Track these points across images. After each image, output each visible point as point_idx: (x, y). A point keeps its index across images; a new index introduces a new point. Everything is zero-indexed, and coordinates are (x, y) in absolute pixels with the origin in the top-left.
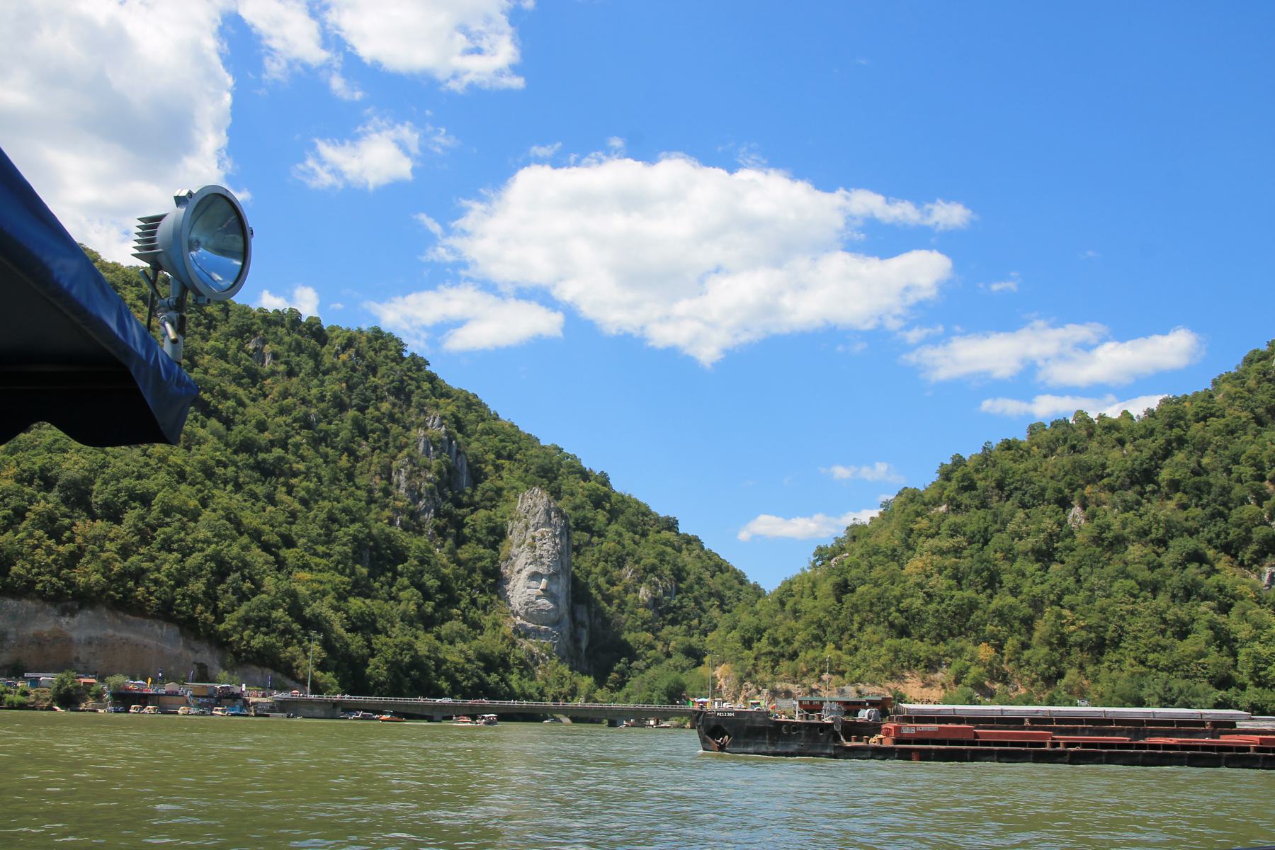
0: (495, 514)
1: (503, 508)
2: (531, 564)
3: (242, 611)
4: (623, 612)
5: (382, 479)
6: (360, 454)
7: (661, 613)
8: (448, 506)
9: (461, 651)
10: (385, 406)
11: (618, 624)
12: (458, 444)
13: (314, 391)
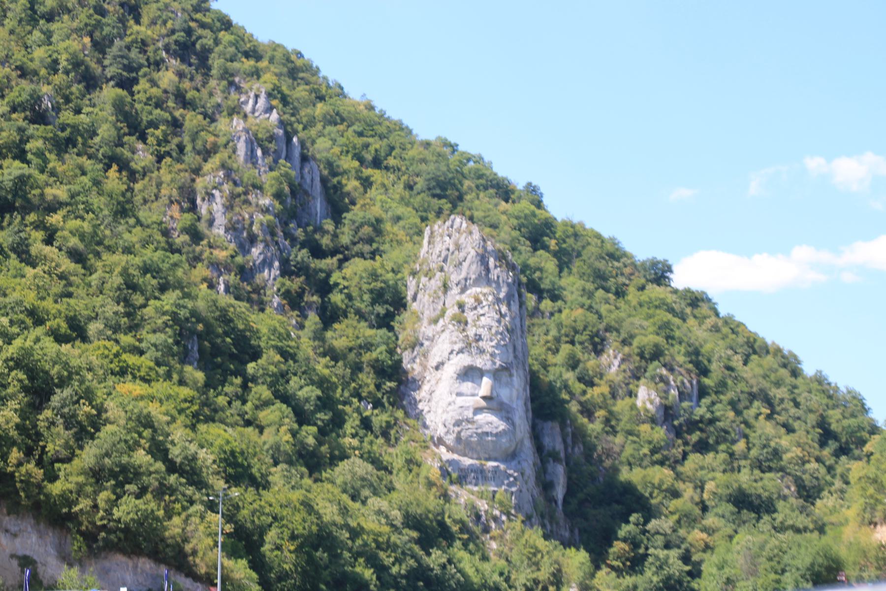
0: (383, 266)
1: (392, 256)
2: (461, 351)
3: (88, 455)
4: (615, 432)
5: (182, 210)
6: (136, 166)
7: (678, 432)
8: (303, 254)
9: (379, 512)
10: (167, 78)
11: (609, 453)
12: (302, 143)
13: (39, 53)
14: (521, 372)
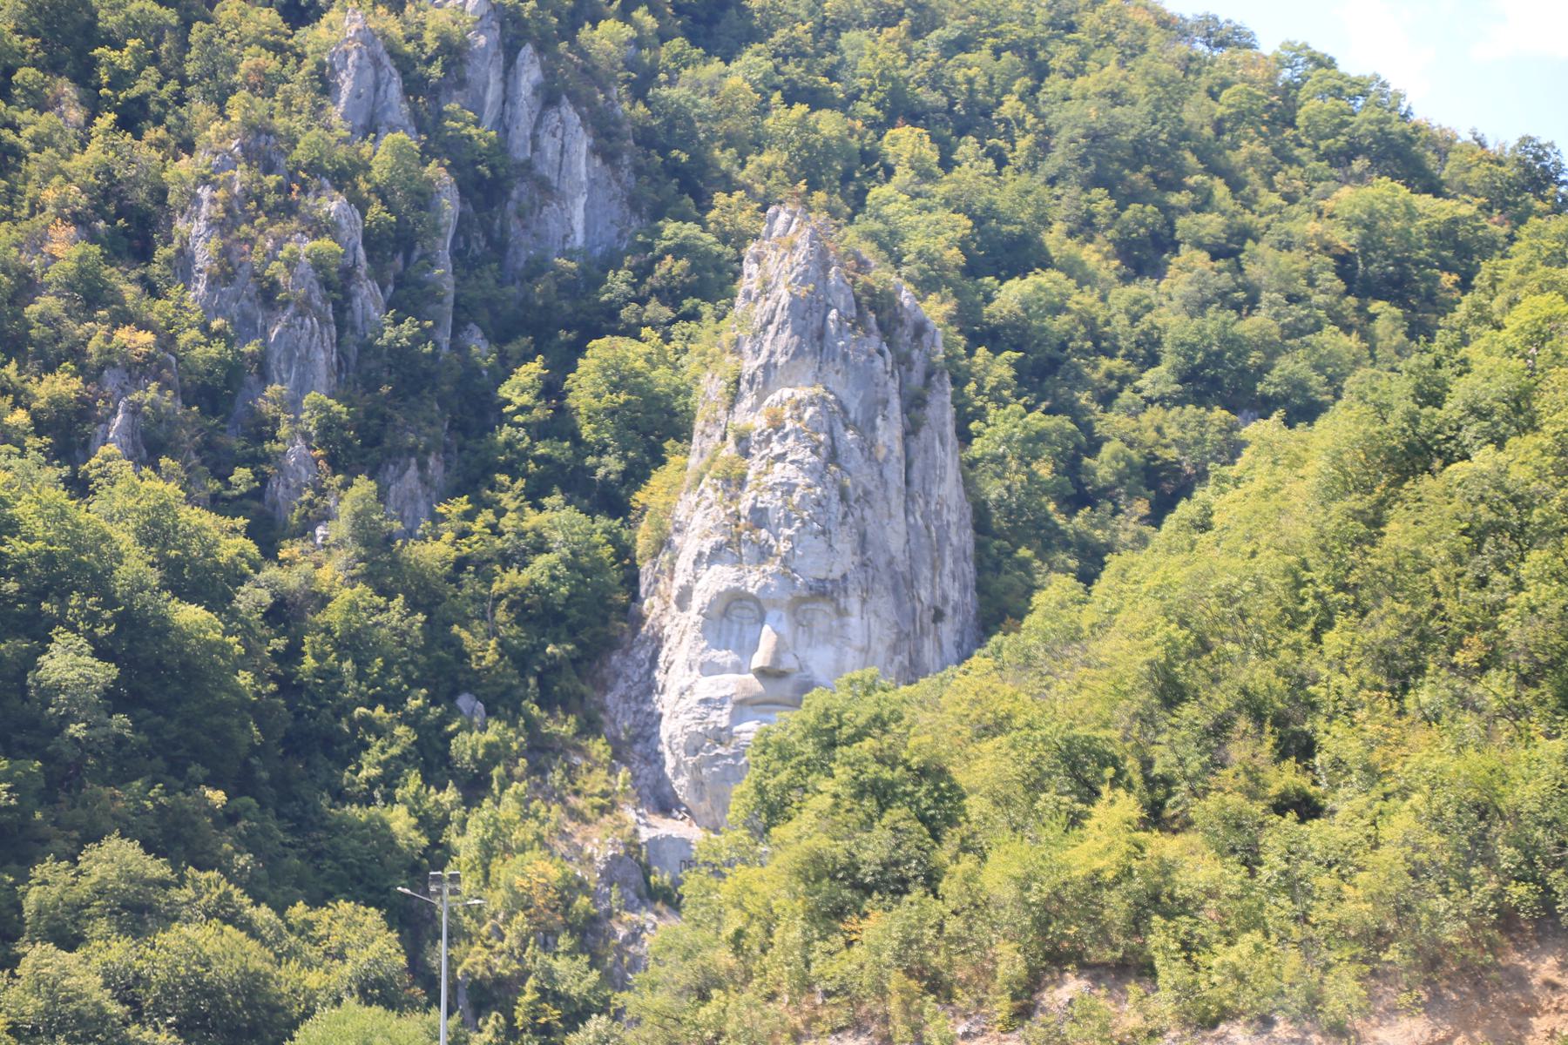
2: (716, 555)
14: (884, 603)
